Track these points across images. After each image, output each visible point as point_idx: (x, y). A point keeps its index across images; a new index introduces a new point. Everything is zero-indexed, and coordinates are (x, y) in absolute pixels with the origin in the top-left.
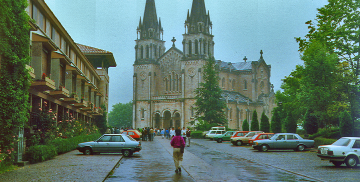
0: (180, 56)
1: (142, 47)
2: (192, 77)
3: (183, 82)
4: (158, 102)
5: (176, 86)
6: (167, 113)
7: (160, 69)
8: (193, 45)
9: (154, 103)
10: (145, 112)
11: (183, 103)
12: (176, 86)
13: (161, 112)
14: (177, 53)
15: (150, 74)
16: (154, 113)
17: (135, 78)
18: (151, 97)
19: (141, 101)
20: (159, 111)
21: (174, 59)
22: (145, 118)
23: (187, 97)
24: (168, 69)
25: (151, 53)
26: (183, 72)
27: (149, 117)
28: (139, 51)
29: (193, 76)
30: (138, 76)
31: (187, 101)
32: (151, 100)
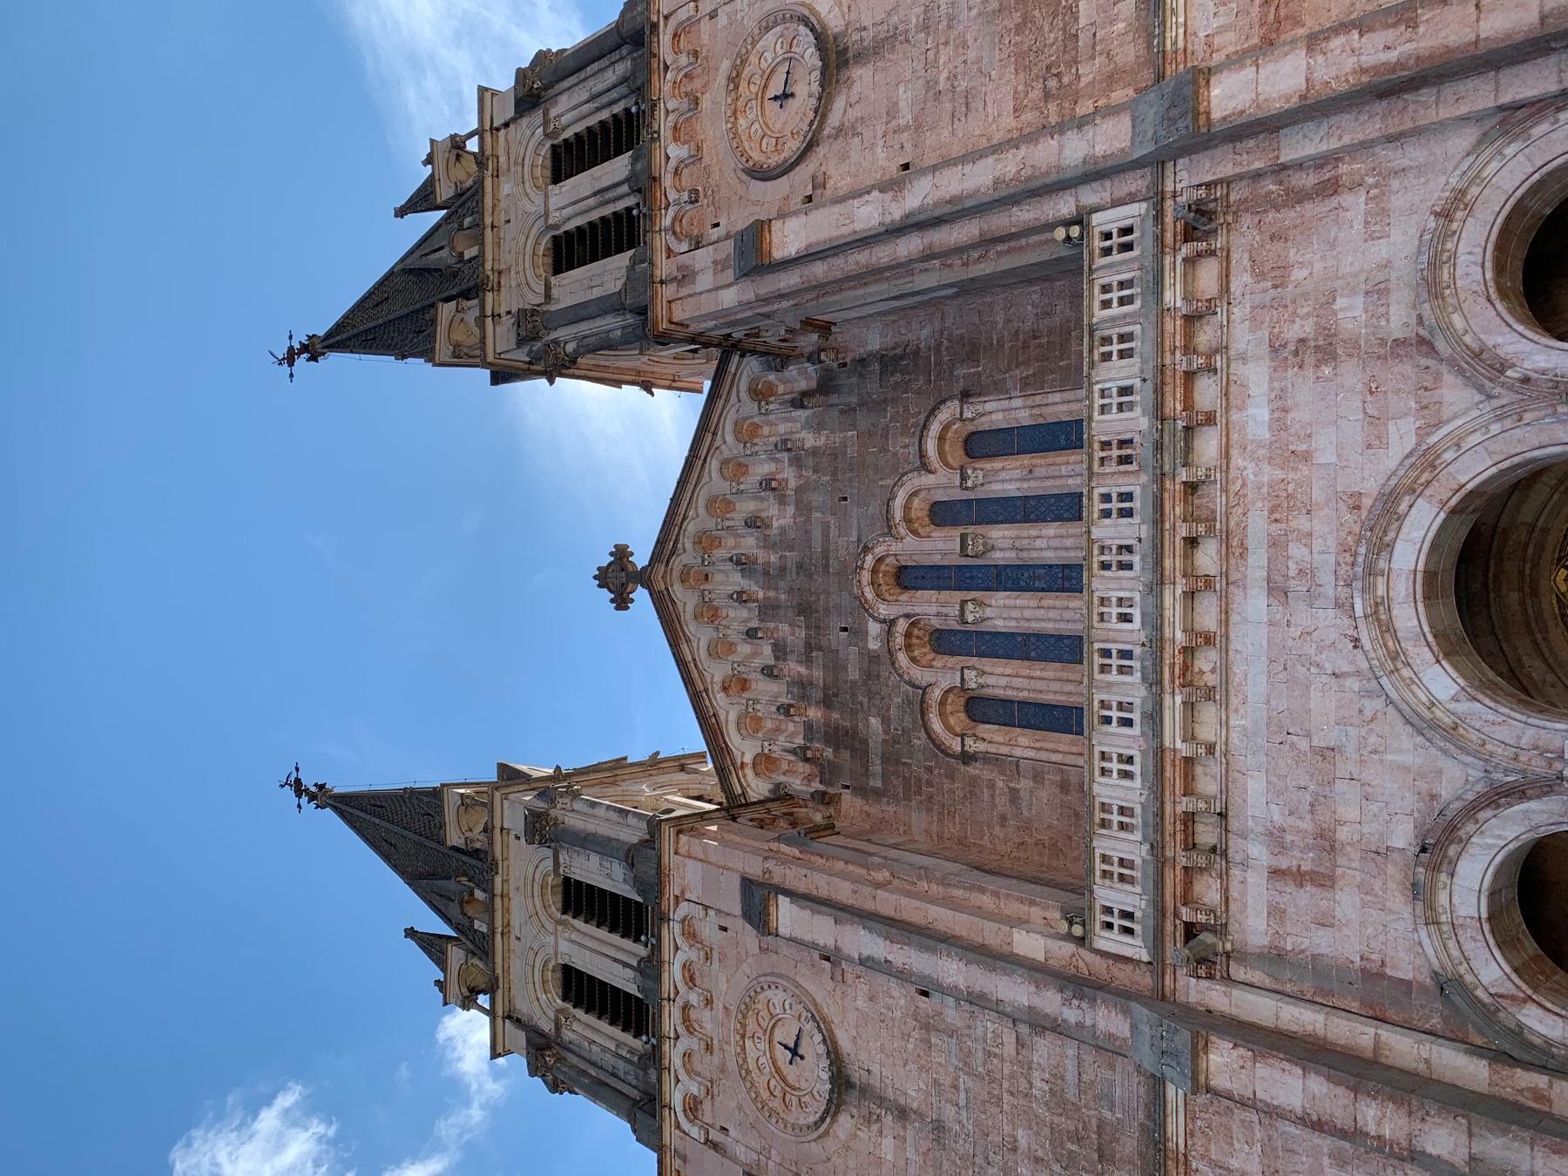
24: (835, 665)
29: (822, 40)
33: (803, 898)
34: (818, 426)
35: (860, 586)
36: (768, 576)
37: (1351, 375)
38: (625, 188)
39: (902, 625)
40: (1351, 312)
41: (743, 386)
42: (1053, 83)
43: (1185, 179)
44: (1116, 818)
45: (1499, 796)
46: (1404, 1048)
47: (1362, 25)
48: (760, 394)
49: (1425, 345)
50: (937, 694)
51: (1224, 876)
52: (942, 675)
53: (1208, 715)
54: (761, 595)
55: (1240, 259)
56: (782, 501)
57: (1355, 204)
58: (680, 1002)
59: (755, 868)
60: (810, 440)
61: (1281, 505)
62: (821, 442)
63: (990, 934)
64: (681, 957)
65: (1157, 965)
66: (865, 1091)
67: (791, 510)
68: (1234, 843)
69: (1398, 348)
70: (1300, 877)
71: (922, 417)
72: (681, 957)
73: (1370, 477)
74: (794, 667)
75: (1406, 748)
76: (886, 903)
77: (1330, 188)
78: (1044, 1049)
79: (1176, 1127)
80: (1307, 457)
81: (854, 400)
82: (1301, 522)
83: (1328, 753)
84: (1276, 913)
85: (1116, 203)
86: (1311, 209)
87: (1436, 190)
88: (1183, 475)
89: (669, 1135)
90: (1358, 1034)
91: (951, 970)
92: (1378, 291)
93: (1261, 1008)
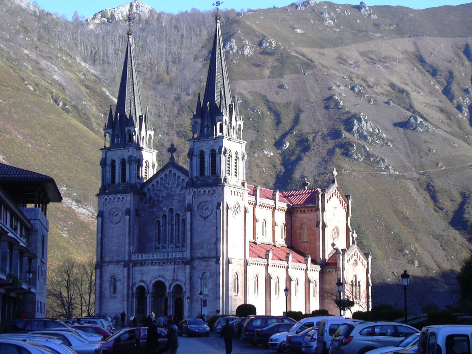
0: (183, 180)
1: (113, 162)
2: (206, 218)
3: (188, 227)
4: (142, 263)
6: (159, 286)
7: (145, 203)
8: (207, 159)
9: (135, 265)
10: (118, 284)
11: (188, 267)
13: (148, 283)
14: (178, 173)
15: (128, 212)
16: (134, 284)
17: (100, 219)
19: (110, 262)
20: (143, 281)
22: (119, 295)
23: (198, 254)
25: (130, 173)
26: (190, 208)
27: (125, 292)
28: (108, 169)
30: (106, 215)
32: (130, 261)
33: (130, 219)
36: (171, 188)
39: (166, 213)
40: (176, 274)
45: (147, 286)
46: (131, 280)
50: (159, 219)
56: (180, 191)
57: (183, 275)
59: (132, 209)
63: (131, 243)
67: (179, 192)
68: (142, 267)
69: (174, 278)
73: (166, 276)
76: (132, 229)
78: (124, 249)
79: (121, 263)
83: (148, 274)
89: (102, 196)
90: (131, 277)
91: (127, 241)
93: (131, 270)
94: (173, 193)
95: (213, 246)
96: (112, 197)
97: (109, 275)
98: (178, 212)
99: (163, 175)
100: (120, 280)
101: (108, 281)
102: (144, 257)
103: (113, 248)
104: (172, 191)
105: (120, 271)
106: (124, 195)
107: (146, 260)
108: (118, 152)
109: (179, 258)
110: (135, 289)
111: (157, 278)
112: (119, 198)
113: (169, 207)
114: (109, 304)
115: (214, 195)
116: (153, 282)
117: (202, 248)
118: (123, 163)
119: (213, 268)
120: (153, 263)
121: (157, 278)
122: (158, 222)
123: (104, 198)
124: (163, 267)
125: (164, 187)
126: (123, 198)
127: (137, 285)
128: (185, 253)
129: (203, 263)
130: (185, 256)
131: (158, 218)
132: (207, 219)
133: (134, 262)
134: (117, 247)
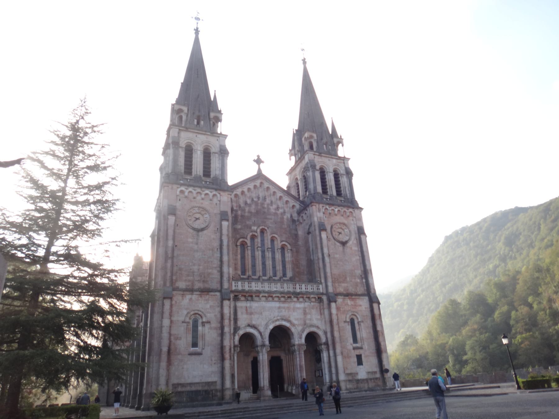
0: (281, 198)
2: (344, 244)
4: (250, 296)
5: (269, 263)
8: (330, 178)
9: (236, 298)
12: (269, 263)
13: (262, 329)
16: (236, 329)
18: (229, 280)
20: (254, 327)
21: (265, 199)
23: (341, 290)
26: (322, 228)
31: (340, 300)
34: (287, 219)
35: (262, 226)
37: (302, 317)
38: (331, 193)
39: (256, 234)
40: (309, 317)
41: (295, 204)
42: (336, 280)
43: (325, 298)
44: (250, 285)
45: (261, 333)
47: (338, 320)
48: (293, 206)
49: (305, 324)
50: (246, 240)
51: (245, 301)
52: (248, 242)
53: (264, 299)
54: (259, 202)
55: (315, 303)
56: (275, 209)
57: (319, 317)
58: (201, 192)
60: (285, 217)
61: (289, 308)
62: (285, 220)
64: (210, 193)
65: (232, 292)
66: (198, 235)
67: (274, 211)
70: (247, 310)
71: (288, 242)
72: (210, 193)
73: (292, 319)
74: (247, 209)
75: (264, 323)
77: (321, 314)
80: (294, 311)
81: (291, 227)
82: (287, 311)
83: (261, 313)
84: (241, 307)
85: (322, 288)
86: (319, 312)
87: (320, 326)
88: (293, 297)
92: (310, 320)
94: (266, 210)
95: (359, 281)
96: (193, 191)
97: (185, 312)
98: (274, 235)
99: (251, 186)
100: (209, 322)
101: (183, 322)
102: (255, 286)
103: (195, 268)
104: (264, 208)
105: (208, 306)
106: (215, 192)
107: (259, 292)
108: (199, 136)
109: (313, 293)
110: (237, 338)
111: (278, 320)
112: (206, 194)
113: (261, 228)
114: (185, 366)
115: (351, 218)
116: (271, 327)
117: (345, 281)
118: (207, 155)
119: (364, 309)
120: (270, 296)
121: (278, 320)
122: (243, 245)
123: (179, 190)
124: (286, 305)
125: (252, 200)
126: (214, 195)
127: (241, 332)
128: (321, 286)
129: (349, 302)
130: (321, 291)
131: (243, 238)
132: (345, 245)
133: (236, 294)
134: (201, 267)
